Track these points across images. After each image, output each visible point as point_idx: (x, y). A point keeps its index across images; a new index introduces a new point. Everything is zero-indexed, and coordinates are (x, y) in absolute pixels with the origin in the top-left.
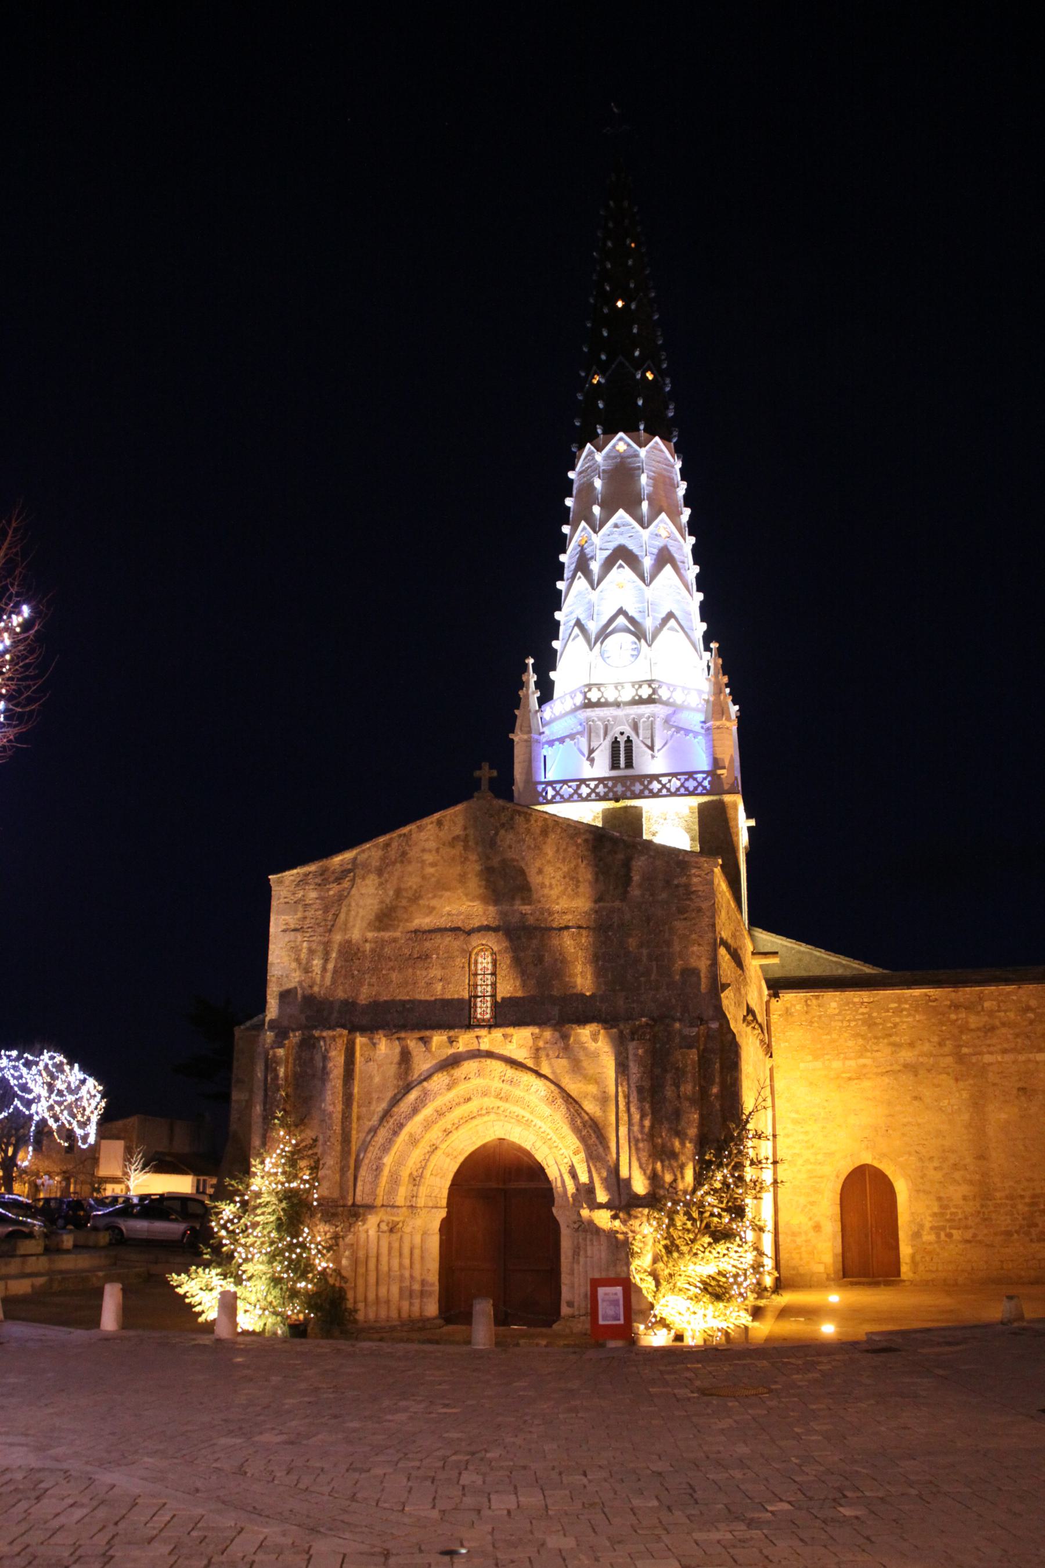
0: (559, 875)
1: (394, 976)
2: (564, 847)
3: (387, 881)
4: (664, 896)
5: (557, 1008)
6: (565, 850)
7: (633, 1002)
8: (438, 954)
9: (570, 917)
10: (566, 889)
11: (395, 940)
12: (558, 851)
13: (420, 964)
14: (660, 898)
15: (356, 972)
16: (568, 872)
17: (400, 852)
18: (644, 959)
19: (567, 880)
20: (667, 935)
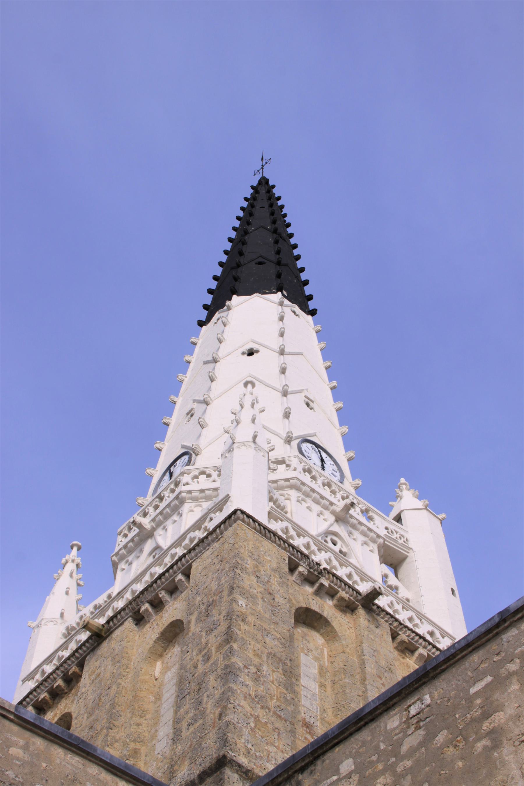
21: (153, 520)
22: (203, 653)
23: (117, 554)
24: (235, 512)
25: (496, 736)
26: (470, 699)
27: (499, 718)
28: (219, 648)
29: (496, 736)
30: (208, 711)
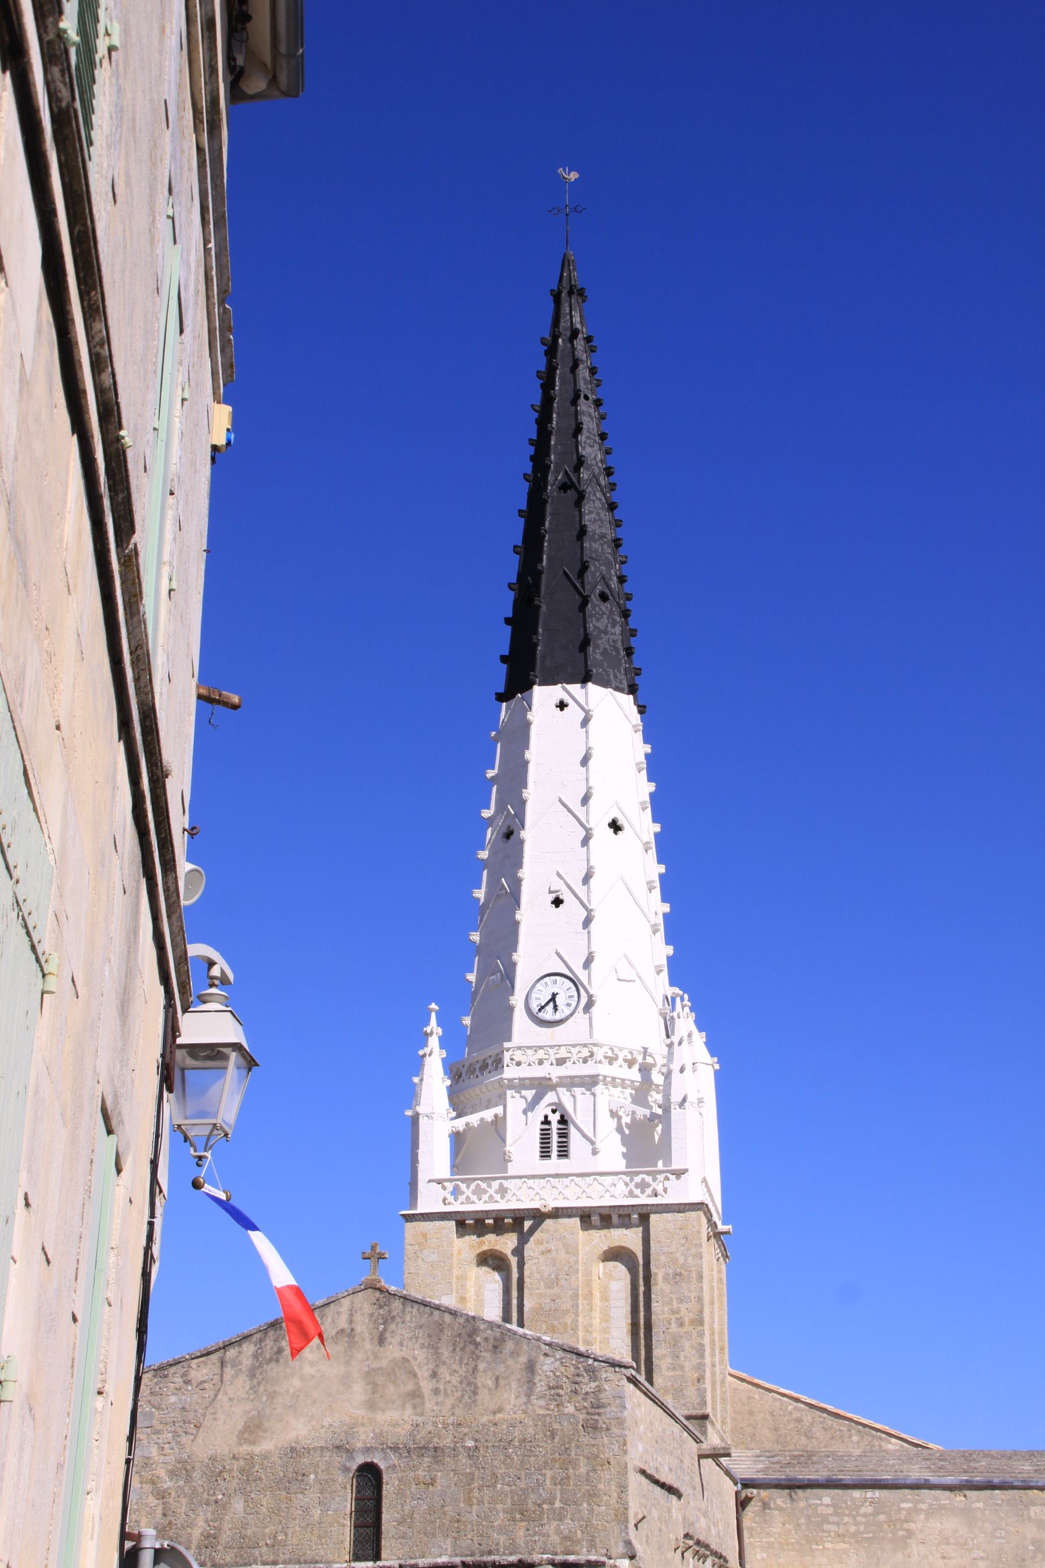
0: (455, 1380)
1: (267, 1501)
2: (462, 1345)
3: (259, 1384)
4: (570, 1409)
5: (449, 1541)
6: (462, 1349)
7: (536, 1533)
8: (316, 1473)
9: (466, 1430)
10: (463, 1396)
11: (265, 1456)
12: (454, 1350)
13: (294, 1487)
14: (566, 1411)
15: (220, 1497)
16: (465, 1377)
17: (275, 1349)
18: (548, 1482)
19: (464, 1385)
20: (573, 1453)
21: (560, 1078)
22: (677, 1316)
23: (510, 1080)
24: (703, 1204)
25: (910, 1534)
26: (900, 1509)
27: (912, 1526)
28: (692, 1322)
29: (910, 1534)
30: (687, 1369)
